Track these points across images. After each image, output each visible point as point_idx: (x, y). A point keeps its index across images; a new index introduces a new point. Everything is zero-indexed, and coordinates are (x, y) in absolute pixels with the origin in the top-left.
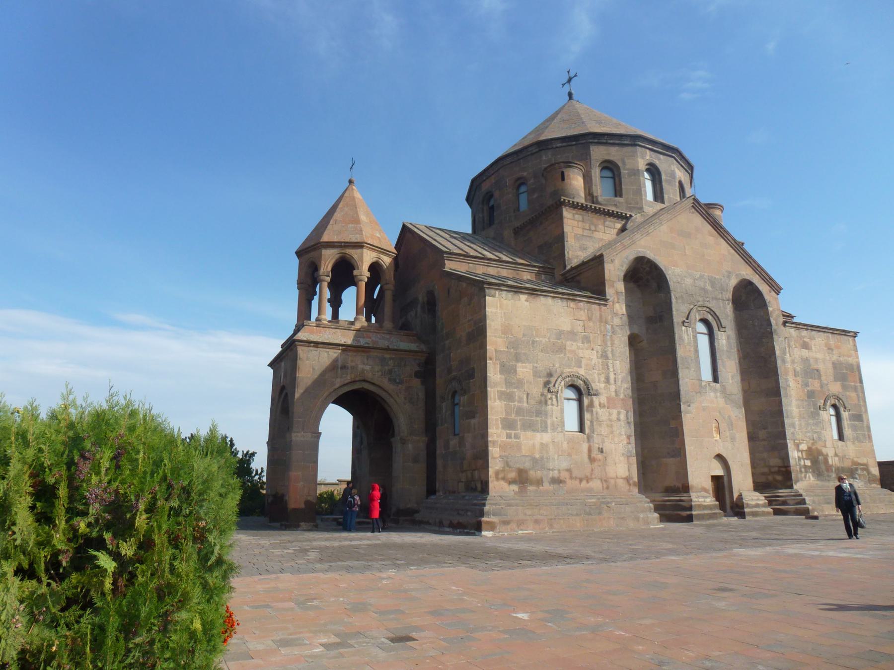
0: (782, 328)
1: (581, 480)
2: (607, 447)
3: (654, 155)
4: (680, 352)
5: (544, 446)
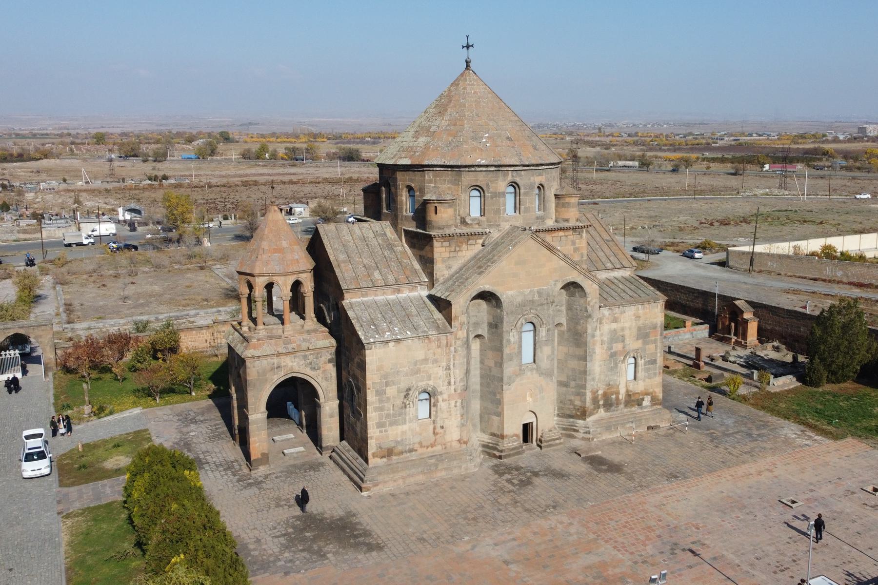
1: (428, 447)
2: (447, 423)
3: (515, 174)
4: (507, 351)
5: (403, 433)
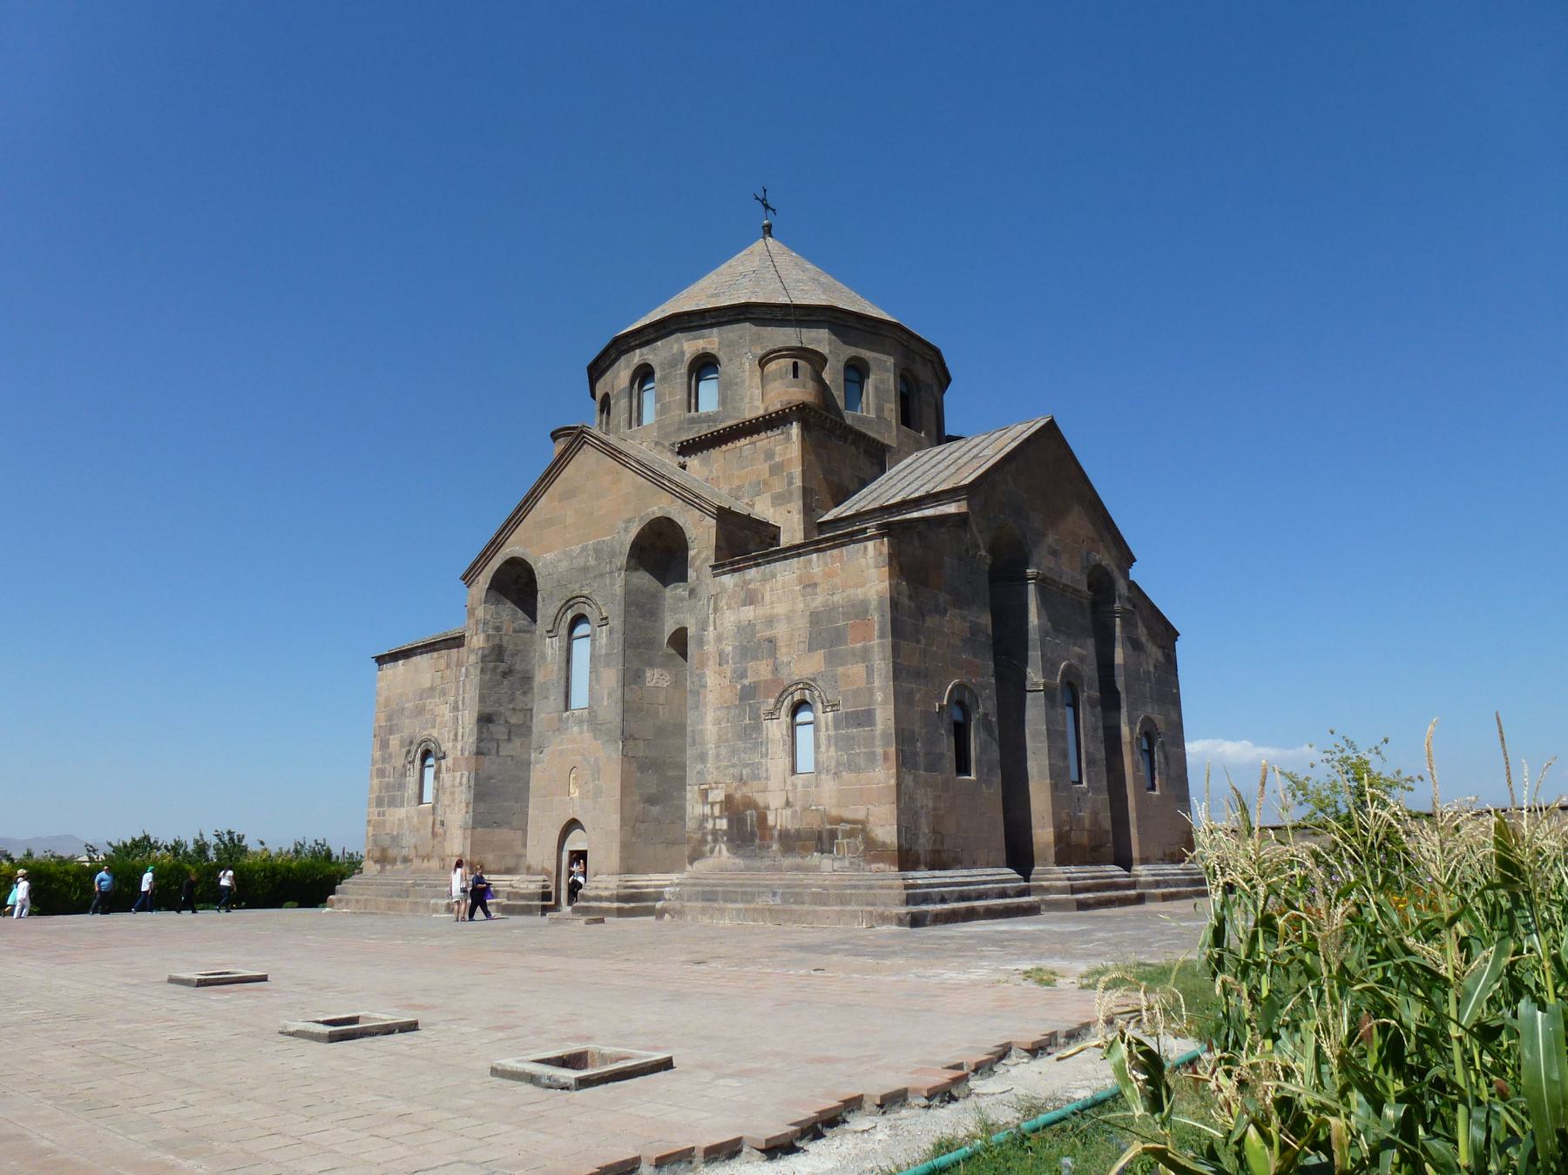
0: (709, 580)
3: (645, 350)
